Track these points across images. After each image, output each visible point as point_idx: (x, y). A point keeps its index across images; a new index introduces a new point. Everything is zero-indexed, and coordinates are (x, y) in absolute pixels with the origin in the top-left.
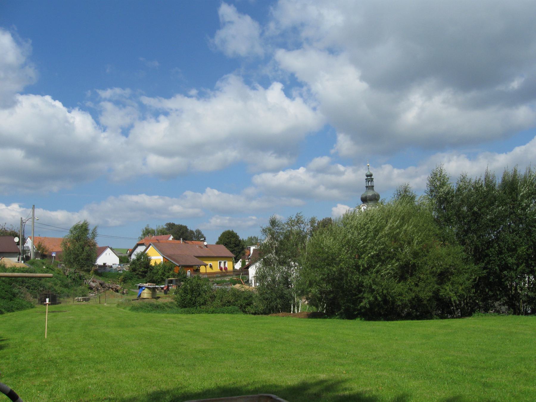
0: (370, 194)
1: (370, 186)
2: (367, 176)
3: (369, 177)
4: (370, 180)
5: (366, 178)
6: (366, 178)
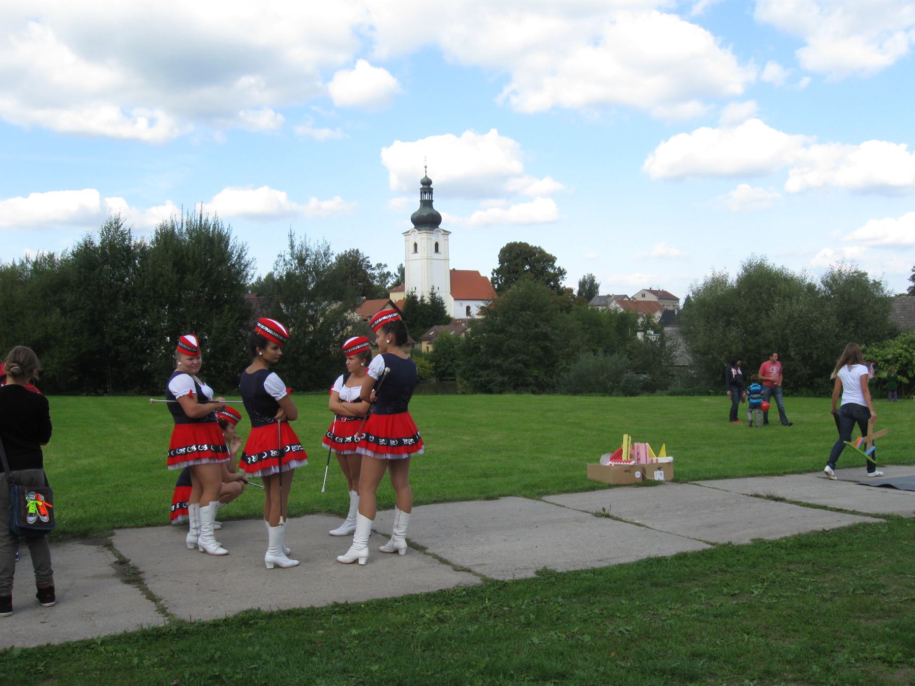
0: (425, 214)
1: (425, 201)
2: (423, 183)
3: (427, 186)
4: (427, 191)
5: (421, 186)
6: (421, 186)
